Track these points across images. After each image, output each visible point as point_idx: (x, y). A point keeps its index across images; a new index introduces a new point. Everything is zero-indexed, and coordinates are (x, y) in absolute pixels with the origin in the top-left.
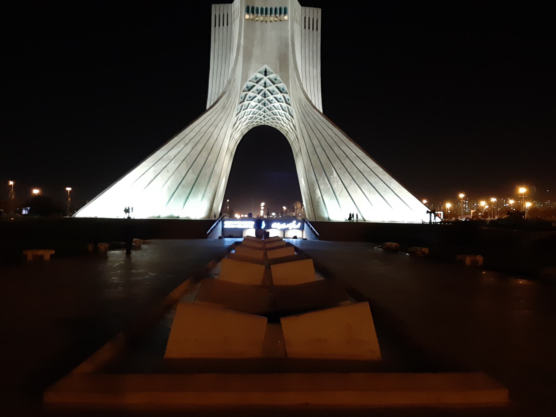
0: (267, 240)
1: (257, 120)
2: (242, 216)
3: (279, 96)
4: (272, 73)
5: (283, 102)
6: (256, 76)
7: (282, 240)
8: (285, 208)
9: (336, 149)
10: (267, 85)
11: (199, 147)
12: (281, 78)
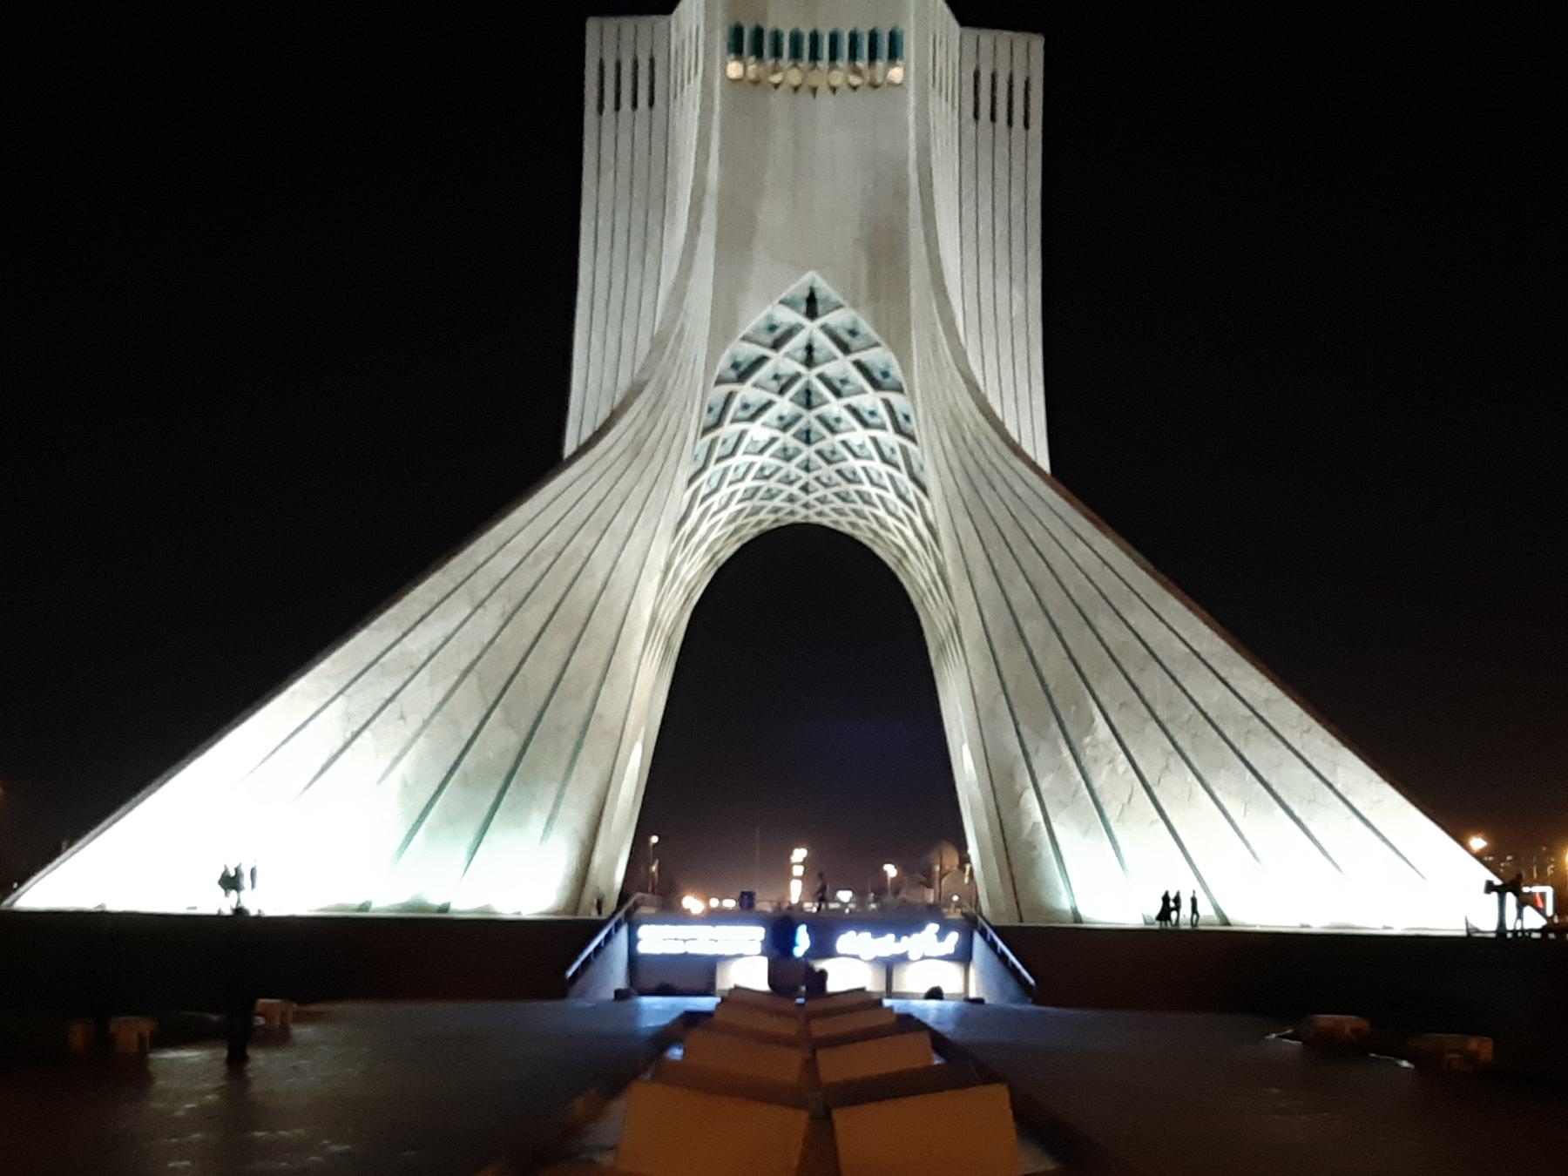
0: (817, 1005)
1: (777, 502)
2: (714, 903)
3: (870, 400)
4: (839, 307)
5: (883, 427)
6: (769, 317)
7: (879, 1003)
8: (891, 870)
9: (1105, 623)
10: (816, 354)
11: (533, 616)
12: (877, 325)
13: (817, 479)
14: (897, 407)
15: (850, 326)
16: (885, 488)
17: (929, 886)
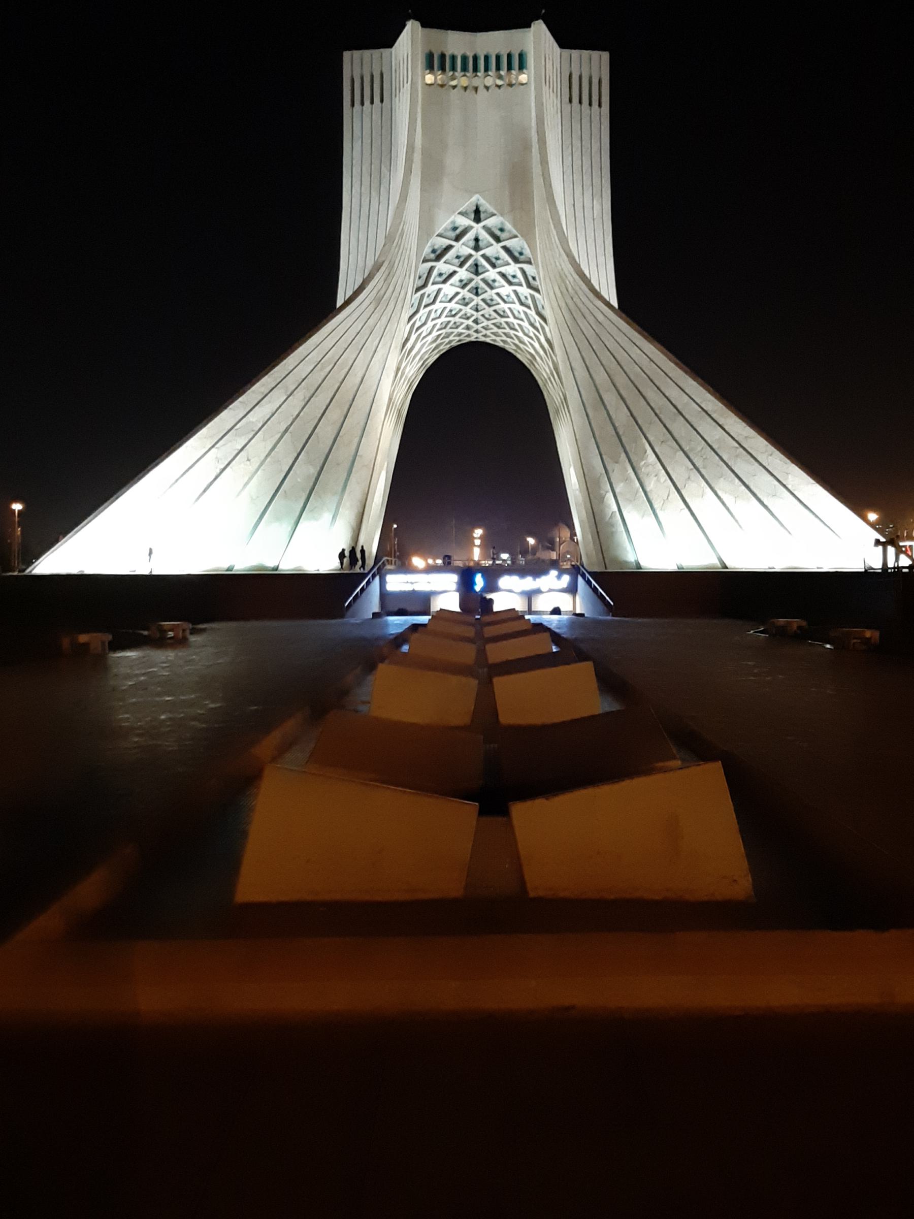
1: (460, 330)
2: (430, 561)
3: (512, 269)
4: (494, 215)
5: (520, 285)
6: (453, 222)
7: (523, 616)
8: (531, 541)
10: (481, 243)
13: (483, 315)
14: (528, 273)
15: (500, 226)
16: (522, 320)
17: (553, 550)
